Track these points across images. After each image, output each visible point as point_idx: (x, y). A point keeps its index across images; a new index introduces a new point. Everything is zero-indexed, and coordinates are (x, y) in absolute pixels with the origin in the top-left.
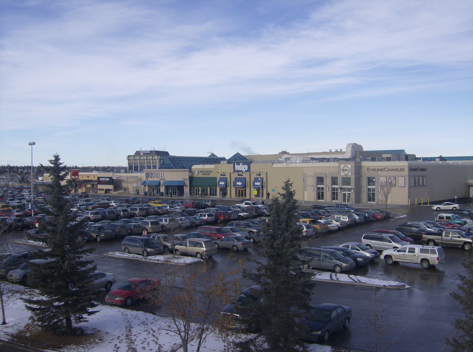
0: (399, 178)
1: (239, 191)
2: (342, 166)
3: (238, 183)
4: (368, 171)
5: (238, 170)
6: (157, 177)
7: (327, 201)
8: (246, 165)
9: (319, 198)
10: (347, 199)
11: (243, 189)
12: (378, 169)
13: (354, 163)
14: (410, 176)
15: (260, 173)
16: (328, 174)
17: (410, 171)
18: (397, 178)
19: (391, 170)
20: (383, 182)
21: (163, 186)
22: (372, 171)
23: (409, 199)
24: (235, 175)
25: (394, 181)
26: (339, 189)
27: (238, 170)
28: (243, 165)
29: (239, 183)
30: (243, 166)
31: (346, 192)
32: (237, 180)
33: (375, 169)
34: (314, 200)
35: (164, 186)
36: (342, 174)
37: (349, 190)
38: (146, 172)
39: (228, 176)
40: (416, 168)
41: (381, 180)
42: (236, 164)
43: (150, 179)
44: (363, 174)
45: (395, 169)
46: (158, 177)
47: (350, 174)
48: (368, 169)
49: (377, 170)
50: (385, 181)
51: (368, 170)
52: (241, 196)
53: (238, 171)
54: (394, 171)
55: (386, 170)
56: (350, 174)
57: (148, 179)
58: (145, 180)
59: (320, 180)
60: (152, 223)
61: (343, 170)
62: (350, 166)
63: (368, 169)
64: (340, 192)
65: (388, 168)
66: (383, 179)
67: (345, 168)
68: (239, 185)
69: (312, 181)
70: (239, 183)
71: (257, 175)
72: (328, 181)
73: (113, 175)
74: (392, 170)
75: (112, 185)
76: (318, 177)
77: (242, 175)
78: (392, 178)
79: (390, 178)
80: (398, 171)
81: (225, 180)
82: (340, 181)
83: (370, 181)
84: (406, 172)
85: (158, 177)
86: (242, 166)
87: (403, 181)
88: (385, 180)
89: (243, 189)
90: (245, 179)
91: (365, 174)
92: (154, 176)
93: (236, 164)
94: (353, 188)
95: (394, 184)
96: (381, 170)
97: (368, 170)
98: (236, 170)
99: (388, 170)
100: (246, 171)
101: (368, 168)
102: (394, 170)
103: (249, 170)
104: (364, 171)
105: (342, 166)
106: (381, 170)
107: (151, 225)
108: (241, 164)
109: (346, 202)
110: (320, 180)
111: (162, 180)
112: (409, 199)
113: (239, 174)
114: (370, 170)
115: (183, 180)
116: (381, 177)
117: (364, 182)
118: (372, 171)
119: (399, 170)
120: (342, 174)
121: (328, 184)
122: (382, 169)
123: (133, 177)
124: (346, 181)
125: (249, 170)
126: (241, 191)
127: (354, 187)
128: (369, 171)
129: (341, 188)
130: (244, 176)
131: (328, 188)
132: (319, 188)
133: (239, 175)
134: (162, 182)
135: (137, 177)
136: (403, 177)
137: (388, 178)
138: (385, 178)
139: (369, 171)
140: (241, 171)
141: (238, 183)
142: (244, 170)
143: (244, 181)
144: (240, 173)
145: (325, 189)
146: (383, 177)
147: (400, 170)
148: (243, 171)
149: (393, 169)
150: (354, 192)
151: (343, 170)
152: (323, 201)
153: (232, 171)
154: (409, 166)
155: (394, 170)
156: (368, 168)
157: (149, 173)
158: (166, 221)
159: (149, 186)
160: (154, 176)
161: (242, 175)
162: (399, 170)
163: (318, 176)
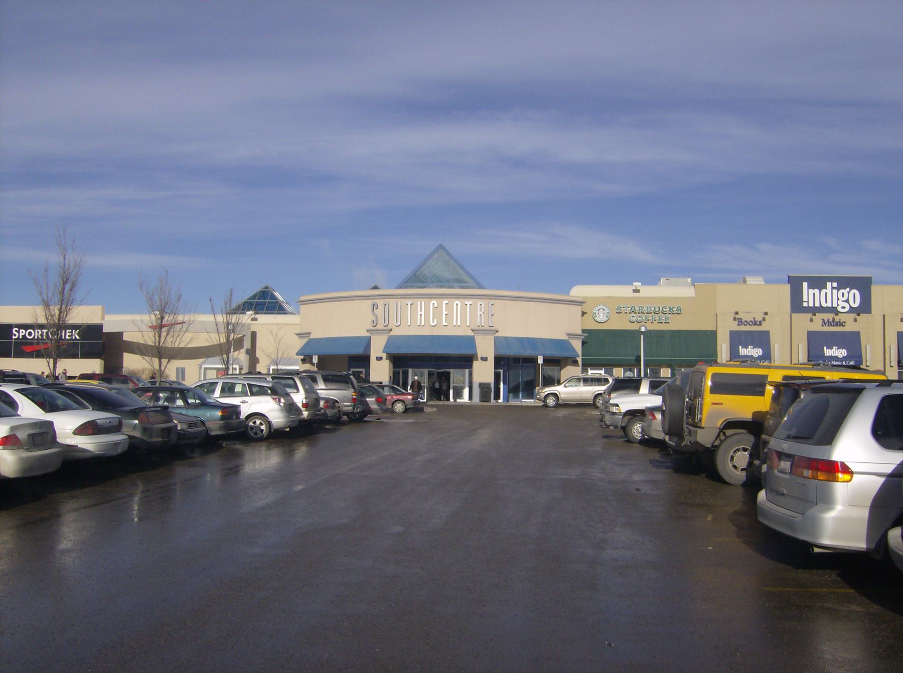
28: (838, 289)
42: (805, 284)
75: (99, 360)
77: (842, 324)
93: (805, 284)
98: (805, 305)
100: (852, 310)
108: (829, 284)
115: (565, 338)
125: (865, 307)
140: (833, 310)
148: (839, 309)
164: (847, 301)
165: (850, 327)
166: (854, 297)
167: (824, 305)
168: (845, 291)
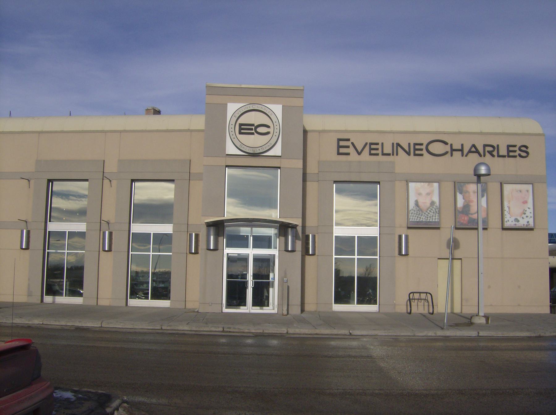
4: (339, 154)
7: (102, 303)
9: (51, 290)
10: (254, 289)
16: (111, 167)
18: (503, 184)
19: (462, 150)
22: (359, 154)
26: (212, 230)
31: (251, 252)
33: (379, 147)
34: (30, 294)
36: (231, 149)
41: (412, 199)
45: (485, 146)
47: (277, 151)
48: (342, 143)
50: (433, 203)
51: (342, 150)
54: (480, 156)
55: (437, 148)
63: (342, 143)
65: (446, 143)
74: (470, 151)
80: (499, 156)
87: (525, 202)
97: (342, 150)
99: (448, 148)
101: (339, 140)
102: (477, 152)
114: (351, 150)
116: (411, 185)
118: (359, 154)
120: (231, 149)
122: (415, 144)
128: (348, 154)
131: (111, 234)
139: (348, 154)
147: (509, 151)
149: (474, 146)
152: (77, 301)
155: (477, 152)
162: (503, 151)
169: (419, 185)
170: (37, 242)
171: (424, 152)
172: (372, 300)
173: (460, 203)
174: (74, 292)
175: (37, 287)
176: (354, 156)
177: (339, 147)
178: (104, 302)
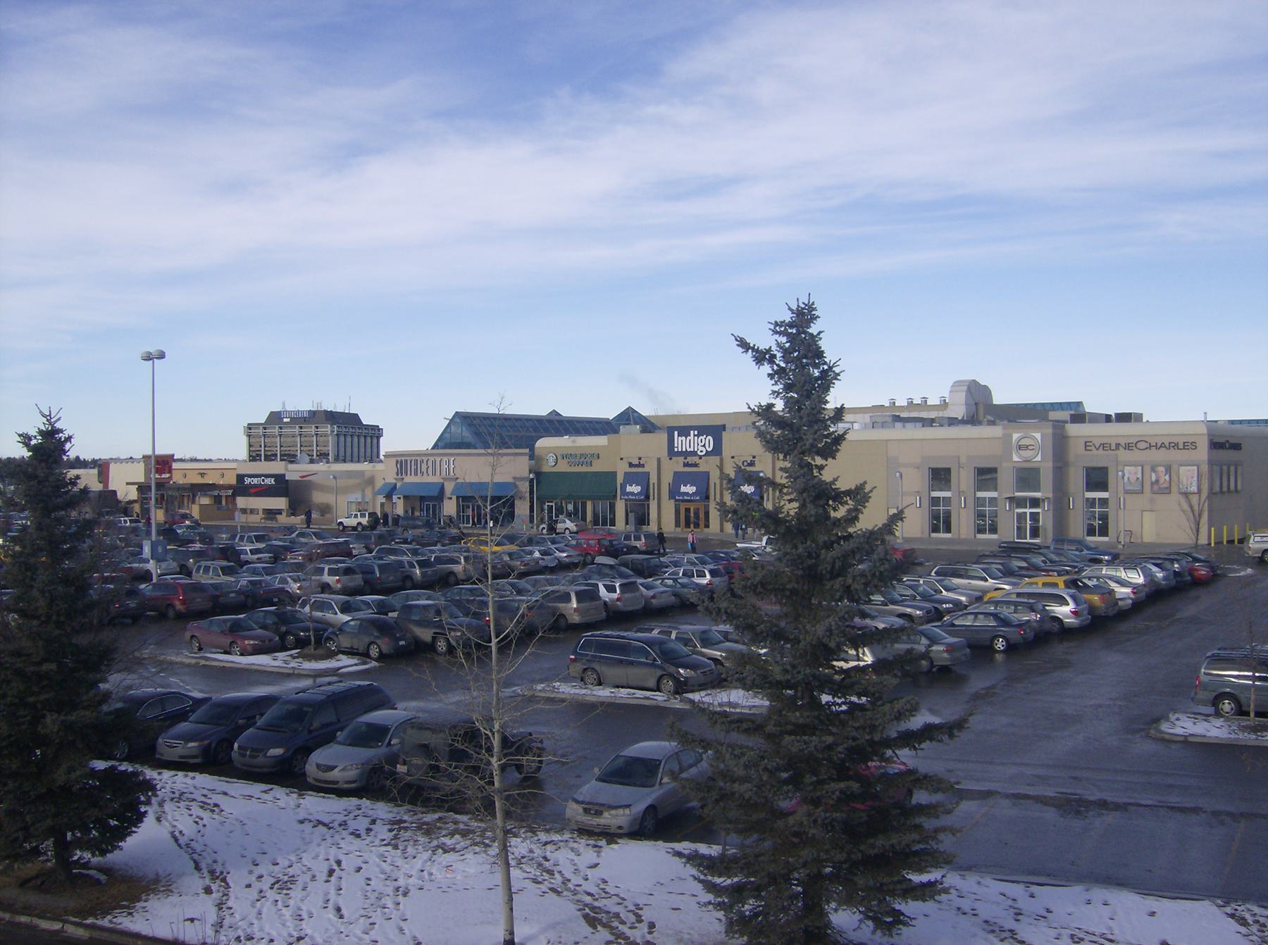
0: (1182, 469)
1: (687, 510)
2: (1015, 436)
3: (683, 489)
5: (684, 450)
6: (434, 474)
8: (709, 437)
9: (935, 529)
11: (701, 506)
12: (1118, 445)
13: (1051, 426)
14: (1211, 463)
15: (754, 457)
16: (963, 460)
17: (1211, 448)
18: (1174, 467)
19: (1156, 446)
20: (1133, 479)
21: (451, 498)
22: (1097, 449)
23: (1213, 529)
24: (678, 465)
25: (1167, 477)
26: (1008, 501)
27: (684, 450)
28: (698, 436)
29: (690, 489)
30: (701, 437)
31: (1028, 511)
32: (680, 478)
34: (923, 533)
35: (454, 498)
36: (1016, 458)
37: (1035, 503)
38: (399, 459)
39: (651, 468)
40: (1223, 440)
42: (676, 433)
43: (410, 479)
44: (1072, 458)
46: (438, 473)
47: (1039, 458)
48: (1088, 444)
49: (1113, 447)
50: (1138, 478)
51: (1088, 448)
52: (692, 526)
53: (686, 454)
56: (1040, 458)
57: (403, 479)
58: (395, 481)
59: (940, 476)
60: (581, 596)
61: (1020, 447)
62: (1038, 436)
63: (1088, 444)
64: (1010, 510)
66: (1131, 473)
67: (1024, 442)
68: (687, 494)
69: (915, 482)
70: (690, 489)
71: (745, 464)
72: (964, 479)
73: (286, 469)
74: (1161, 446)
76: (933, 469)
77: (696, 465)
78: (1161, 469)
79: (1153, 469)
81: (643, 480)
82: (1006, 479)
83: (1097, 479)
84: (1202, 453)
85: (438, 473)
86: (696, 438)
88: (1140, 476)
89: (701, 506)
90: (706, 475)
91: (1080, 459)
92: (424, 469)
93: (676, 433)
94: (1048, 498)
95: (1166, 485)
96: (1128, 447)
97: (1088, 448)
98: (676, 450)
100: (708, 454)
101: (1086, 442)
103: (717, 450)
104: (1076, 449)
105: (1015, 436)
106: (1128, 447)
107: (578, 602)
108: (692, 432)
109: (1026, 539)
110: (940, 476)
111: (450, 479)
112: (1213, 529)
113: (686, 461)
114: (1093, 448)
115: (511, 480)
117: (1076, 479)
118: (1097, 449)
119: (1181, 446)
120: (1016, 458)
121: (963, 487)
123: (350, 474)
124: (1027, 477)
125: (717, 450)
126: (692, 511)
127: (1050, 495)
129: (1011, 499)
130: (702, 468)
131: (965, 498)
132: (935, 501)
133: (686, 465)
134: (449, 488)
135: (362, 473)
136: (1194, 465)
137: (1147, 468)
138: (1140, 468)
140: (694, 453)
141: (683, 489)
142: (701, 448)
143: (702, 480)
144: (690, 460)
145: (954, 502)
146: (1133, 468)
147: (1184, 446)
148: (699, 453)
150: (1051, 506)
151: (1020, 447)
153: (664, 453)
154: (1209, 435)
155: (1165, 447)
156: (1086, 442)
157: (406, 461)
158: (611, 589)
159: (406, 498)
160: (424, 469)
161: (696, 465)
162: (1181, 446)
163: (933, 466)
164: (704, 446)
165: (703, 468)
166: (709, 442)
167: (688, 450)
168: (703, 438)
169: (1129, 468)
170: (926, 503)
171: (1134, 448)
172: (1106, 534)
173: (1154, 478)
174: (948, 530)
175: (927, 528)
176: (1095, 452)
177: (1086, 446)
178: (963, 537)
